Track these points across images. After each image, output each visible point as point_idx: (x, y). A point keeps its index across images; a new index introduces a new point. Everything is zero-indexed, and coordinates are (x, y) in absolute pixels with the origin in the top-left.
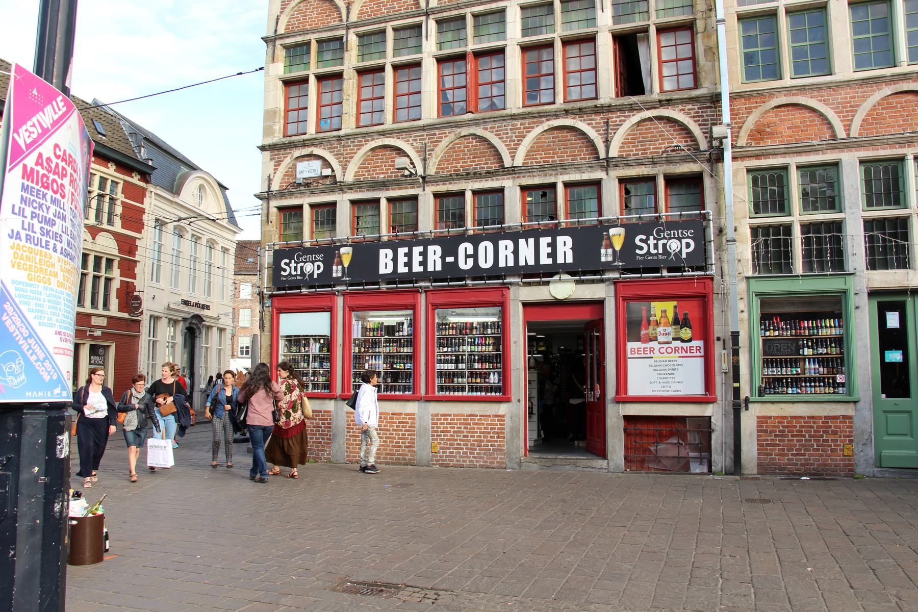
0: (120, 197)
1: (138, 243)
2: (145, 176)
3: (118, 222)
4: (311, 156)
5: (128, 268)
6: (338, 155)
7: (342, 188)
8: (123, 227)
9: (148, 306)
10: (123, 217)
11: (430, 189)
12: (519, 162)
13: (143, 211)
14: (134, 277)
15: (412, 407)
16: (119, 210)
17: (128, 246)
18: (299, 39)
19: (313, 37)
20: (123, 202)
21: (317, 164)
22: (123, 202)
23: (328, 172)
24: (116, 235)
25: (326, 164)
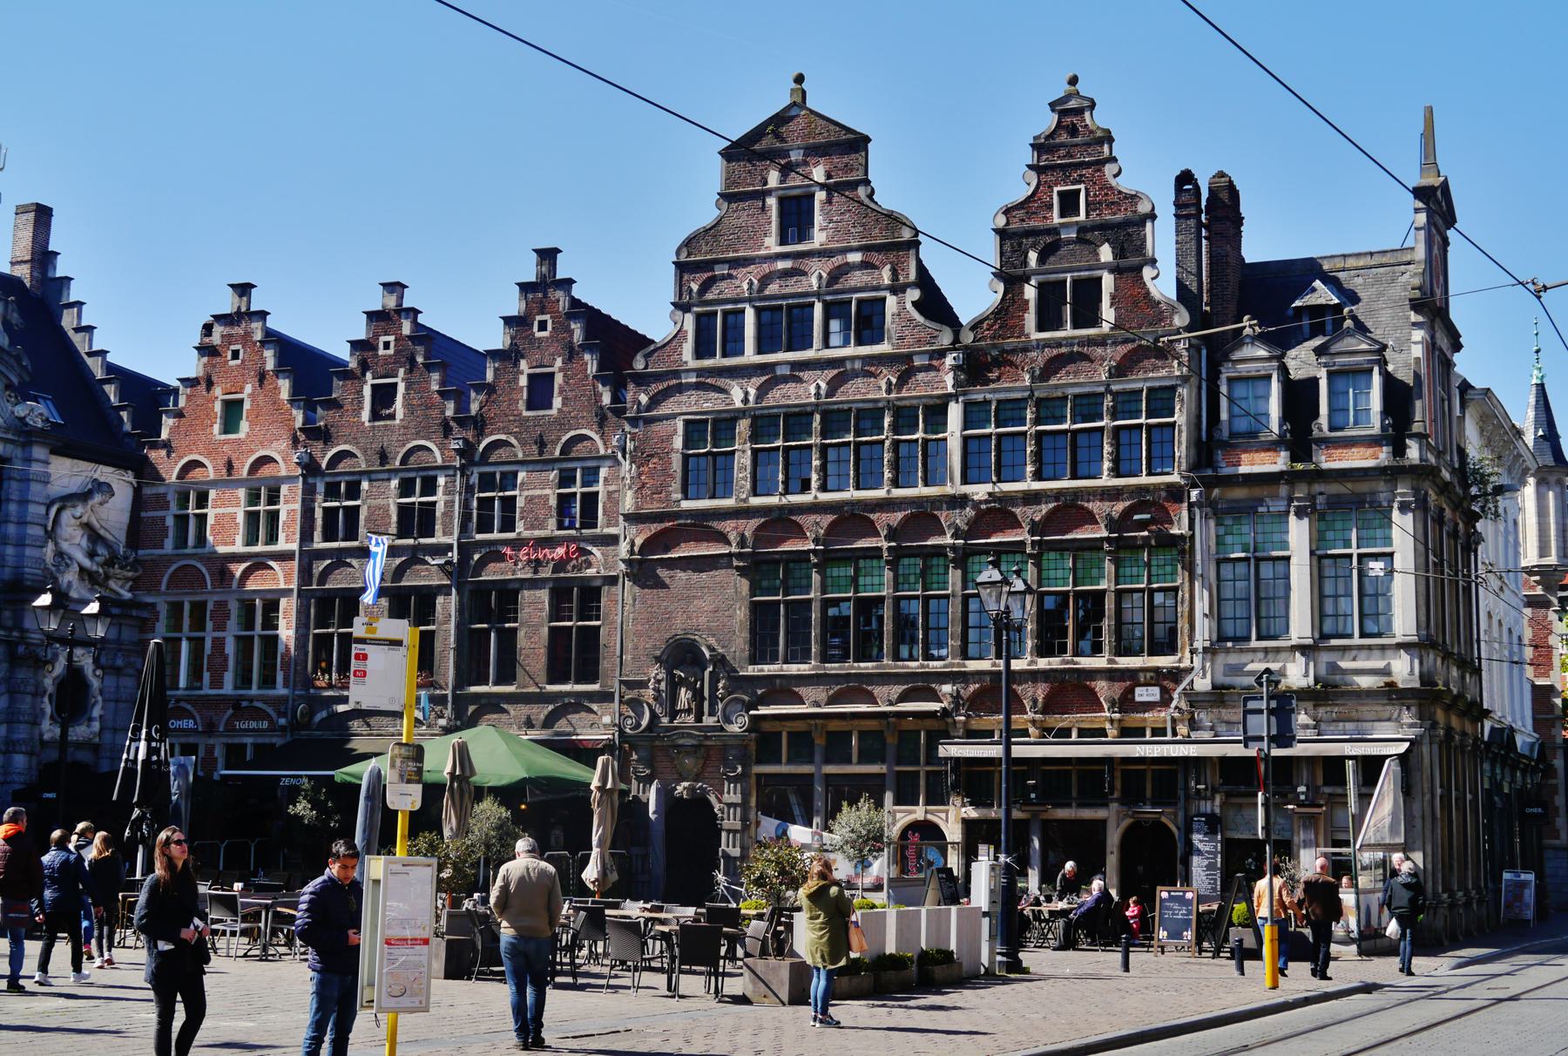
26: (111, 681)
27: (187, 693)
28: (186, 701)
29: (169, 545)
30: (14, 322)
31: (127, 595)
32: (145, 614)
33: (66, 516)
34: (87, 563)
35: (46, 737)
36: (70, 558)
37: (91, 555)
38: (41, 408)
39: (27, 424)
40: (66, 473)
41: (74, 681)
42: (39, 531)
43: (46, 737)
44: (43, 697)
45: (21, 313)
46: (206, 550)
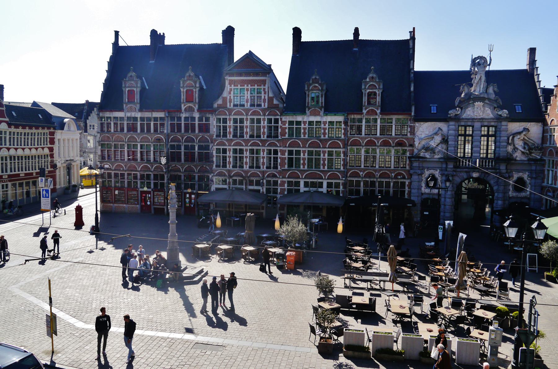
0: (49, 136)
3: (48, 144)
4: (107, 164)
5: (52, 156)
6: (112, 165)
7: (113, 170)
8: (50, 144)
9: (59, 165)
11: (127, 172)
13: (54, 138)
14: (53, 158)
15: (125, 205)
16: (48, 140)
17: (51, 149)
20: (49, 138)
21: (108, 166)
22: (49, 138)
23: (110, 167)
24: (49, 148)
25: (110, 166)
26: (533, 181)
27: (550, 185)
28: (550, 188)
29: (548, 145)
30: (496, 90)
31: (539, 157)
32: (543, 163)
33: (515, 138)
34: (523, 150)
35: (510, 196)
36: (517, 149)
37: (524, 148)
38: (506, 111)
39: (502, 116)
40: (515, 127)
41: (520, 181)
42: (505, 144)
43: (510, 196)
44: (509, 186)
45: (498, 88)
46: (555, 145)
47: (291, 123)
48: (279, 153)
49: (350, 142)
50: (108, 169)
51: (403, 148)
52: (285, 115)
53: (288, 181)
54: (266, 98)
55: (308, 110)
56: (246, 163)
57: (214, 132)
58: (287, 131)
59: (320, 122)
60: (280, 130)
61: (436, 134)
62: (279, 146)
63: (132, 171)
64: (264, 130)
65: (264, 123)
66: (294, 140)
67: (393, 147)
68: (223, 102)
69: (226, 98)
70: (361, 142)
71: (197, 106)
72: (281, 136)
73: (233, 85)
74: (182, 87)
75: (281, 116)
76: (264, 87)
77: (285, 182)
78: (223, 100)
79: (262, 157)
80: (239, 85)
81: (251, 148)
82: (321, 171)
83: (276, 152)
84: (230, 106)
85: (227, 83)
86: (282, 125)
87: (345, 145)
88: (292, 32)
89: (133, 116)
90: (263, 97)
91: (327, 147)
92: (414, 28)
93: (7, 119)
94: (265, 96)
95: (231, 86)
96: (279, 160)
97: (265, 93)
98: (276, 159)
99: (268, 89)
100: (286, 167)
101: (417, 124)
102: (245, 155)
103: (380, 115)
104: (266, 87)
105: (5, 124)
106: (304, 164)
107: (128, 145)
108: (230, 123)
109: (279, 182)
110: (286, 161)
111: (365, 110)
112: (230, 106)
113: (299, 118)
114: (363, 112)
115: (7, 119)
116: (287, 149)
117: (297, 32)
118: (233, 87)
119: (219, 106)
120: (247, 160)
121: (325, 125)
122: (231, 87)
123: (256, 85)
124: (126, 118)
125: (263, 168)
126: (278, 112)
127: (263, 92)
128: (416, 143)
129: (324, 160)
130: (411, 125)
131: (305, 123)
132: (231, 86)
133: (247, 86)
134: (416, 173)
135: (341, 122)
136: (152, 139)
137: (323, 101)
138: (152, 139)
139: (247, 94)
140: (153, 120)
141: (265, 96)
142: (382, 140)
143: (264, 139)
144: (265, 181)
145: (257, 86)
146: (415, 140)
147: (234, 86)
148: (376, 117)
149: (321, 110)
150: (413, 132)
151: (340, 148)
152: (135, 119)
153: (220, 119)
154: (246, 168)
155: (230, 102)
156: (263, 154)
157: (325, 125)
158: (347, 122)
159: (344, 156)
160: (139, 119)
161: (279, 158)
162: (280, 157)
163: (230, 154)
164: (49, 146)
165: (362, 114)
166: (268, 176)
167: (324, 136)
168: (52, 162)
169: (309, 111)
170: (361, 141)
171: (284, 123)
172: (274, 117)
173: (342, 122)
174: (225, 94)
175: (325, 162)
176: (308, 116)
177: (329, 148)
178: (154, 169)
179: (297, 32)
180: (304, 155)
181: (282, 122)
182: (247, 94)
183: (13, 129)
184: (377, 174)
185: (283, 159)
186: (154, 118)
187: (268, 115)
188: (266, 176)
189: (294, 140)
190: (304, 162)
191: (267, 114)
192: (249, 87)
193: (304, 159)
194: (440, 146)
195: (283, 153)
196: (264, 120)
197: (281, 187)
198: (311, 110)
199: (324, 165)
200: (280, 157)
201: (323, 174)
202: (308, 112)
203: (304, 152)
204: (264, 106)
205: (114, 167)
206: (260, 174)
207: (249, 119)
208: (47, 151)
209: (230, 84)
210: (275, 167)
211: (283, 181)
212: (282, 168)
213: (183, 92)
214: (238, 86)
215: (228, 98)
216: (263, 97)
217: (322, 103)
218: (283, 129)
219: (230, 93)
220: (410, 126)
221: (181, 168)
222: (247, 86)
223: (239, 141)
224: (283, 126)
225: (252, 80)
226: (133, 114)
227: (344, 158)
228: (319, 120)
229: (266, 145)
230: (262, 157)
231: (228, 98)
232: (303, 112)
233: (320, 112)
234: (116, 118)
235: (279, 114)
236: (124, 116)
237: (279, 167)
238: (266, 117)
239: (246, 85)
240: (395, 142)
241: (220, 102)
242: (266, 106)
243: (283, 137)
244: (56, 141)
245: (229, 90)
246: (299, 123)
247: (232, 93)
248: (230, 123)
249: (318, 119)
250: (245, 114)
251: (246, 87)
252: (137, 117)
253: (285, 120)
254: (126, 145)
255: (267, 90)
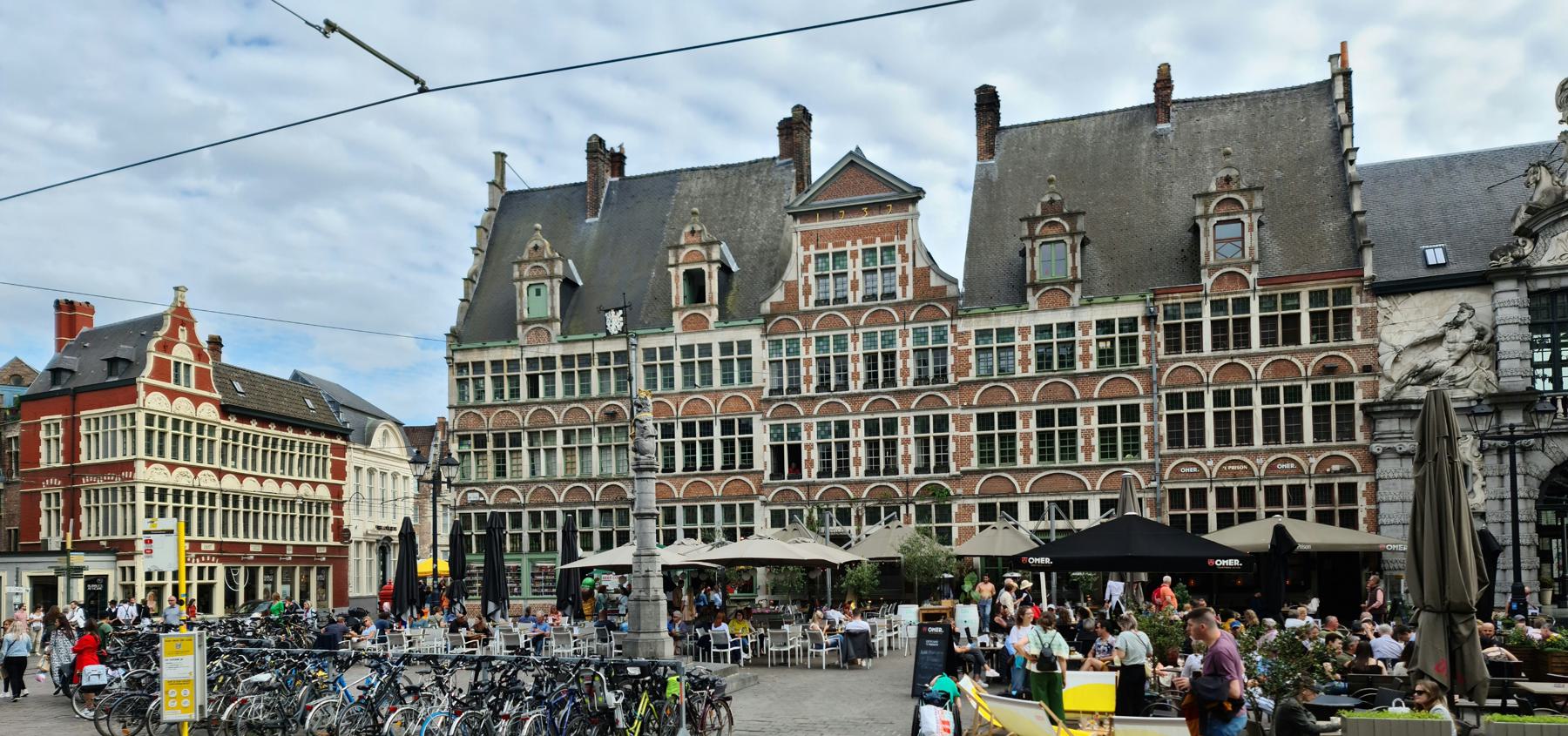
0: (330, 456)
1: (344, 488)
2: (345, 437)
3: (329, 475)
4: (474, 491)
6: (487, 492)
7: (488, 507)
8: (333, 478)
10: (333, 471)
12: (562, 500)
13: (345, 463)
14: (342, 514)
16: (329, 465)
17: (336, 491)
18: (465, 433)
19: (472, 433)
20: (332, 460)
21: (477, 494)
22: (332, 460)
47: (983, 334)
48: (952, 426)
49: (1165, 376)
50: (474, 504)
51: (1341, 380)
52: (964, 317)
53: (980, 505)
54: (910, 271)
55: (1034, 295)
56: (857, 459)
57: (764, 380)
58: (972, 359)
59: (1072, 325)
60: (951, 360)
61: (1456, 324)
62: (950, 404)
63: (541, 505)
64: (905, 362)
65: (904, 345)
66: (993, 384)
67: (1307, 379)
68: (786, 296)
69: (796, 282)
70: (1203, 373)
71: (715, 312)
72: (957, 374)
73: (812, 247)
74: (672, 266)
75: (952, 319)
76: (902, 243)
77: (970, 508)
78: (786, 290)
79: (903, 439)
80: (830, 245)
81: (868, 417)
82: (1080, 469)
83: (942, 423)
84: (807, 304)
85: (796, 240)
86: (956, 344)
87: (1152, 385)
88: (973, 99)
89: (544, 355)
90: (899, 272)
91: (1096, 395)
92: (1344, 45)
93: (218, 396)
94: (904, 268)
95: (807, 249)
96: (952, 447)
97: (905, 258)
98: (942, 443)
99: (914, 247)
100: (974, 464)
101: (1384, 303)
102: (852, 438)
103: (1258, 288)
104: (908, 242)
105: (213, 408)
106: (1027, 453)
107: (529, 433)
108: (807, 353)
109: (955, 509)
110: (974, 447)
111: (1210, 276)
112: (807, 304)
113: (1006, 321)
114: (1203, 282)
115: (218, 396)
116: (974, 412)
117: (988, 101)
118: (813, 251)
119: (777, 309)
120: (858, 453)
121: (1086, 333)
122: (807, 253)
123: (878, 239)
124: (524, 362)
125: (907, 472)
126: (944, 309)
127: (898, 257)
128: (1386, 360)
129: (1088, 435)
130: (1363, 305)
131: (1024, 331)
132: (807, 249)
133: (854, 243)
134: (1392, 450)
135: (1135, 319)
136: (594, 413)
137: (1078, 263)
138: (594, 413)
139: (854, 267)
140: (596, 361)
141: (904, 268)
142: (1269, 360)
143: (905, 388)
144: (912, 509)
145: (882, 241)
146: (1380, 350)
147: (817, 247)
148: (1247, 295)
149: (1073, 291)
150: (1371, 329)
151: (1137, 396)
152: (549, 361)
153: (779, 342)
154: (857, 474)
155: (807, 293)
156: (906, 433)
157: (1086, 333)
158: (1155, 317)
159: (1151, 418)
160: (559, 362)
161: (951, 438)
162: (954, 437)
163: (809, 437)
164: (329, 479)
165: (1201, 288)
166: (920, 496)
167: (1086, 366)
168: (338, 525)
169: (1038, 295)
170: (1199, 369)
171: (962, 337)
172: (933, 324)
173: (1140, 321)
174: (791, 274)
175: (1090, 442)
176: (1035, 311)
177: (1101, 399)
178: (602, 494)
179: (988, 101)
180: (1026, 425)
181: (958, 336)
182: (854, 267)
183: (232, 423)
184: (1259, 461)
185: (963, 443)
186: (598, 354)
187: (916, 320)
188: (914, 495)
189: (993, 384)
190: (1026, 446)
191: (911, 318)
192: (860, 246)
193: (1026, 437)
194: (1469, 360)
195: (963, 424)
196: (904, 334)
197: (960, 524)
198: (1041, 292)
199: (1088, 450)
200: (954, 437)
201: (1085, 475)
202: (1032, 300)
203: (1026, 416)
204: (904, 295)
205: (493, 497)
206: (897, 489)
207: (861, 336)
208: (323, 493)
209: (806, 246)
210: (942, 466)
211: (964, 506)
212: (962, 469)
213: (677, 276)
214: (826, 247)
215: (801, 282)
216: (899, 272)
217: (1074, 268)
218: (962, 356)
219: (805, 269)
220: (1361, 311)
221: (674, 488)
222: (854, 243)
223: (836, 400)
224: (959, 348)
225: (866, 226)
226: (543, 351)
227: (1150, 424)
228: (1070, 320)
229: (913, 407)
230: (903, 439)
231: (801, 282)
232: (1019, 301)
233: (1069, 296)
234: (497, 365)
235: (948, 314)
236: (519, 357)
237: (952, 465)
238: (910, 327)
239: (849, 243)
240: (1313, 363)
241: (778, 296)
242: (910, 295)
243: (960, 379)
244: (349, 469)
245: (801, 260)
246: (1006, 333)
247: (812, 266)
248: (807, 353)
249: (1064, 316)
250: (849, 324)
251: (849, 247)
252: (554, 357)
253: (967, 329)
254: (525, 436)
255: (909, 250)
